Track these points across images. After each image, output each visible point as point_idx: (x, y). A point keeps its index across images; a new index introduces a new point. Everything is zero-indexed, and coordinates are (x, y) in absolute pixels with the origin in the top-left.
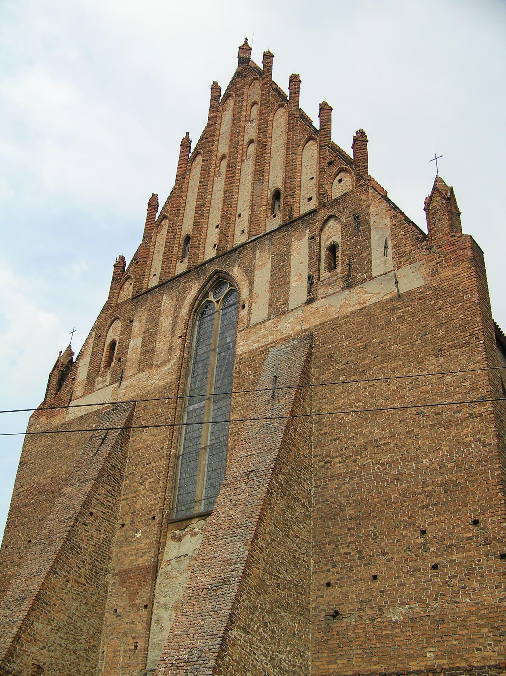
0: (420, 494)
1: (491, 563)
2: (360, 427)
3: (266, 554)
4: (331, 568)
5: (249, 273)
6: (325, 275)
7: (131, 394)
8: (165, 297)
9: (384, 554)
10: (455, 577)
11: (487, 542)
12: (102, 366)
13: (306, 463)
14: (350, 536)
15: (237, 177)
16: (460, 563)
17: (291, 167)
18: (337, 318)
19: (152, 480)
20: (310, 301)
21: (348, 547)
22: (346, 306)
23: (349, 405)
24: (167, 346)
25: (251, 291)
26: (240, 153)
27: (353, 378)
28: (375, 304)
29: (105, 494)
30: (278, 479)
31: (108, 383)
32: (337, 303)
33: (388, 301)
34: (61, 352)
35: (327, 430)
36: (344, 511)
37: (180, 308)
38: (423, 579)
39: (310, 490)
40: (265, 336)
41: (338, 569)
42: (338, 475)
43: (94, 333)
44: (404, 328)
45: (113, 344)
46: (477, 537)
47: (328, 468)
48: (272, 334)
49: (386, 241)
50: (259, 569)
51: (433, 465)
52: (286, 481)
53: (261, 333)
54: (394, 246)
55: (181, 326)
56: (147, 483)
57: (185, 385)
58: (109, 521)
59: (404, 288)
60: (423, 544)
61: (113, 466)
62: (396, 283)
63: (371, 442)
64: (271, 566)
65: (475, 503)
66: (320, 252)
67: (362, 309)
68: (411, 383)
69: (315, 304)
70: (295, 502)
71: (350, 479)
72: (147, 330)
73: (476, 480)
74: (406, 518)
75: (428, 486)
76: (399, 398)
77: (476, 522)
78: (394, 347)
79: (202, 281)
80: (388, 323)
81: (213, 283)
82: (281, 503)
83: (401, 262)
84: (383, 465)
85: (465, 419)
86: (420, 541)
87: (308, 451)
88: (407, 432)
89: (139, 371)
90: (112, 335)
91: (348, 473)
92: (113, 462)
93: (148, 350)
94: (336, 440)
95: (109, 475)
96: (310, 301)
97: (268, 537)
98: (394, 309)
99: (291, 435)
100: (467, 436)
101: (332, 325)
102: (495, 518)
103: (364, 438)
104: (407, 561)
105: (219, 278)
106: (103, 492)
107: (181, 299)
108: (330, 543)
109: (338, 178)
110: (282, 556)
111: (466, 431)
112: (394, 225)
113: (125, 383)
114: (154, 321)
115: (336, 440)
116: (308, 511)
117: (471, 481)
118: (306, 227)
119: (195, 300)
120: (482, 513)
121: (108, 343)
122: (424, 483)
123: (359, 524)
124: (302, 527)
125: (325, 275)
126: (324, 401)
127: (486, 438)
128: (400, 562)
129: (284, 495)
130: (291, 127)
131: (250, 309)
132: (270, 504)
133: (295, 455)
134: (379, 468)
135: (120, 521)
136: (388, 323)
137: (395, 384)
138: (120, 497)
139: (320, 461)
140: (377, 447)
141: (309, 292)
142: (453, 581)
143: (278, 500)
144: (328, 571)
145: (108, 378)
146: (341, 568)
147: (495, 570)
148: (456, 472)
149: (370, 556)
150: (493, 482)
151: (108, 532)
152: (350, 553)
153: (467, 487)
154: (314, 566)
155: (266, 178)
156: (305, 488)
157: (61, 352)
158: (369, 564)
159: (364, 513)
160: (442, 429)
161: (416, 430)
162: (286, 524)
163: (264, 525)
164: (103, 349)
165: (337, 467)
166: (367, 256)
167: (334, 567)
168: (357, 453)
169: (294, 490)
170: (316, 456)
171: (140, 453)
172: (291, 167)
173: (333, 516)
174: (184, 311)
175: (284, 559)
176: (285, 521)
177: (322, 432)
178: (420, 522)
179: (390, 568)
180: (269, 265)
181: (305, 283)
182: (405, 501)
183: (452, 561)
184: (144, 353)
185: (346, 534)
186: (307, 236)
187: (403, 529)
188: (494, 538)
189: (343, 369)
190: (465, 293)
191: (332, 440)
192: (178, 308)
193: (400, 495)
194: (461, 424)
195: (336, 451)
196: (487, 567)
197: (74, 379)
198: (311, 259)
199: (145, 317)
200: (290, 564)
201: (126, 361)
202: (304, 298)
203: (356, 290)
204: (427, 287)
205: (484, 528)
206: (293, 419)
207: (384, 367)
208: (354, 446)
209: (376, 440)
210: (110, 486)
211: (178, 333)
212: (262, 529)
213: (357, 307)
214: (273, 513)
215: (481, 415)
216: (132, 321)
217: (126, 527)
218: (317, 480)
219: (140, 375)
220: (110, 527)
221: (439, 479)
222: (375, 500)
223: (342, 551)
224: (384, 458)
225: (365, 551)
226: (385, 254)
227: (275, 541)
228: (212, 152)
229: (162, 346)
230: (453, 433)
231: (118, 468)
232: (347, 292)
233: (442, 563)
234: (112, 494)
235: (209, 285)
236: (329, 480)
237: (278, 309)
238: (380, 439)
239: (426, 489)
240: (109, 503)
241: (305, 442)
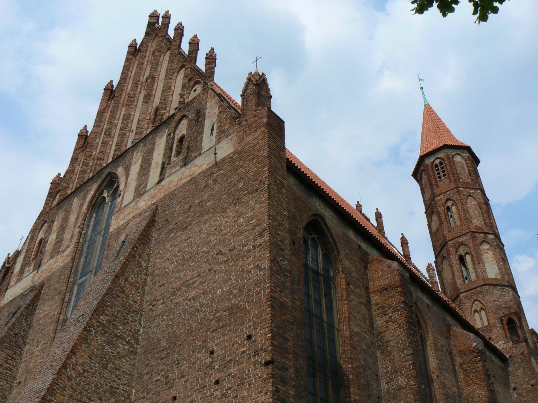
0: (213, 320)
1: (257, 371)
2: (178, 272)
3: (76, 383)
4: (146, 395)
5: (127, 170)
8: (75, 200)
9: (183, 376)
10: (230, 388)
11: (256, 353)
12: (31, 259)
13: (136, 308)
14: (162, 365)
15: (135, 104)
16: (235, 375)
17: (168, 87)
18: (175, 190)
19: (43, 342)
21: (159, 374)
22: (181, 179)
23: (174, 256)
26: (140, 87)
27: (179, 234)
28: (200, 173)
29: (5, 358)
30: (100, 319)
31: (31, 271)
34: (9, 254)
35: (157, 279)
36: (160, 343)
37: (83, 206)
38: (208, 395)
39: (139, 330)
40: (129, 214)
41: (151, 395)
42: (159, 315)
43: (30, 235)
44: (216, 188)
46: (249, 350)
47: (154, 310)
48: (133, 212)
49: (213, 125)
50: (64, 395)
51: (224, 294)
52: (109, 322)
53: (126, 213)
54: (218, 127)
55: (81, 217)
56: (40, 345)
57: (78, 264)
58: (8, 381)
59: (220, 157)
60: (211, 363)
61: (16, 334)
62: (215, 154)
63: (184, 283)
64: (81, 393)
65: (250, 321)
66: (172, 144)
67: (192, 179)
68: (216, 229)
69: (163, 183)
70: (117, 340)
71: (167, 316)
72: (61, 226)
73: (252, 300)
74: (201, 343)
75: (218, 312)
76: (207, 244)
77: (249, 337)
78: (208, 204)
79: (99, 182)
81: (107, 183)
82: (100, 339)
83: (221, 138)
84: (190, 300)
85: (250, 251)
86: (209, 360)
87: (139, 298)
88: (209, 270)
90: (41, 235)
91: (166, 312)
92: (17, 331)
93: (59, 241)
94: (162, 286)
95: (10, 342)
97: (80, 369)
98: (212, 174)
99: (121, 284)
100: (249, 264)
102: (263, 331)
103: (180, 281)
104: (198, 380)
105: (111, 178)
106: (3, 356)
107: (84, 199)
108: (147, 373)
109: (194, 89)
110: (96, 386)
111: (249, 261)
112: (220, 112)
113: (41, 269)
114: (66, 219)
115: (162, 286)
116: (134, 348)
117: (249, 302)
118: (167, 128)
119: (93, 198)
120: (255, 329)
121: (37, 241)
122: (216, 310)
123: (169, 353)
124: (124, 361)
125: (174, 159)
126: (158, 256)
127: (263, 263)
128: (193, 382)
129: (105, 333)
130: (171, 62)
131: (123, 196)
132: (86, 340)
133: (123, 300)
134: (187, 304)
135: (18, 381)
136: (207, 186)
137: (206, 233)
138: (21, 359)
139: (149, 305)
140: (188, 286)
141: (161, 174)
142: (229, 392)
143: (97, 337)
144: (144, 398)
145: (32, 267)
146: (153, 394)
147: (260, 377)
148: (239, 296)
149: (173, 380)
150: (264, 300)
151: (5, 390)
152: (159, 380)
153: (245, 308)
154: (135, 395)
155: (152, 100)
156: (132, 328)
157: (9, 254)
158: (172, 387)
159: (173, 343)
160: (233, 262)
161: (215, 267)
162: (105, 358)
163: (76, 357)
164: (34, 247)
165: (160, 307)
166: (200, 139)
167: (148, 394)
168: (174, 294)
169: (118, 329)
170: (146, 302)
171: (41, 322)
172: (168, 87)
173: (152, 350)
174: (85, 207)
175: (98, 388)
176: (104, 355)
177: (153, 281)
178: (211, 345)
179: (185, 388)
181: (159, 169)
182: (201, 328)
183: (229, 374)
184: (56, 244)
185: (159, 363)
187: (198, 353)
188: (261, 349)
189: (174, 228)
190: (259, 151)
191: (159, 287)
192: (81, 206)
193: (199, 323)
194: (246, 256)
195: (160, 295)
196: (254, 375)
197: (12, 273)
198: (166, 149)
199: (61, 217)
200: (105, 392)
201: (44, 252)
202: (157, 179)
203: (190, 165)
204: (234, 153)
205: (255, 342)
206: (124, 270)
207: (199, 221)
208: (173, 288)
209: (187, 281)
210: (11, 350)
211: (79, 224)
212: (73, 360)
213: (189, 178)
214: (89, 347)
215: (261, 245)
216: (53, 222)
217: (21, 384)
218: (146, 321)
219: (52, 261)
220: (8, 385)
221: (226, 304)
222: (182, 331)
223: (155, 379)
224: (191, 295)
225: (170, 375)
226: (211, 134)
227: (88, 372)
228: (123, 90)
229: (67, 236)
230: (240, 264)
231: (21, 336)
232: (183, 169)
233: (222, 377)
234: (12, 358)
235: (104, 185)
236: (153, 320)
237: (139, 193)
238: (190, 279)
239: (216, 315)
240: (8, 365)
241: (136, 290)
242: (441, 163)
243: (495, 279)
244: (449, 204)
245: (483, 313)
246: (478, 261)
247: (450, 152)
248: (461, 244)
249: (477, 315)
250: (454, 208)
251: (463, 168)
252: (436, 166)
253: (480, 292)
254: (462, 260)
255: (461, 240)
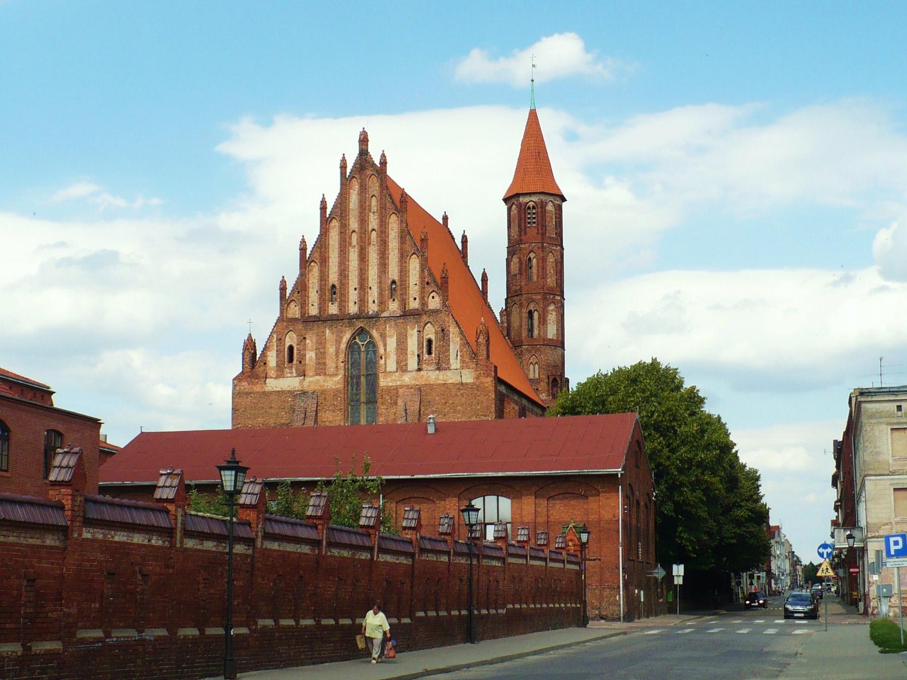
5: (383, 337)
6: (426, 356)
7: (314, 387)
20: (419, 370)
24: (334, 365)
25: (385, 349)
32: (432, 376)
33: (457, 384)
37: (340, 343)
44: (463, 400)
45: (291, 348)
53: (394, 377)
80: (456, 395)
89: (317, 375)
96: (419, 370)
101: (431, 386)
113: (308, 379)
174: (343, 346)
180: (395, 338)
186: (416, 329)
203: (442, 373)
219: (318, 377)
229: (331, 364)
237: (402, 367)
242: (534, 208)
243: (552, 340)
244: (532, 255)
245: (537, 366)
246: (543, 321)
247: (543, 198)
248: (533, 301)
249: (531, 367)
250: (534, 261)
251: (552, 218)
252: (529, 208)
253: (538, 350)
254: (530, 314)
255: (534, 297)
